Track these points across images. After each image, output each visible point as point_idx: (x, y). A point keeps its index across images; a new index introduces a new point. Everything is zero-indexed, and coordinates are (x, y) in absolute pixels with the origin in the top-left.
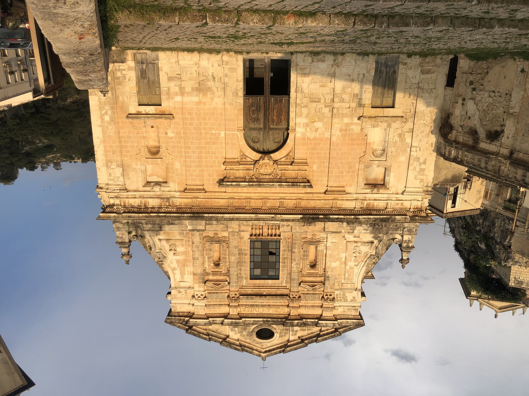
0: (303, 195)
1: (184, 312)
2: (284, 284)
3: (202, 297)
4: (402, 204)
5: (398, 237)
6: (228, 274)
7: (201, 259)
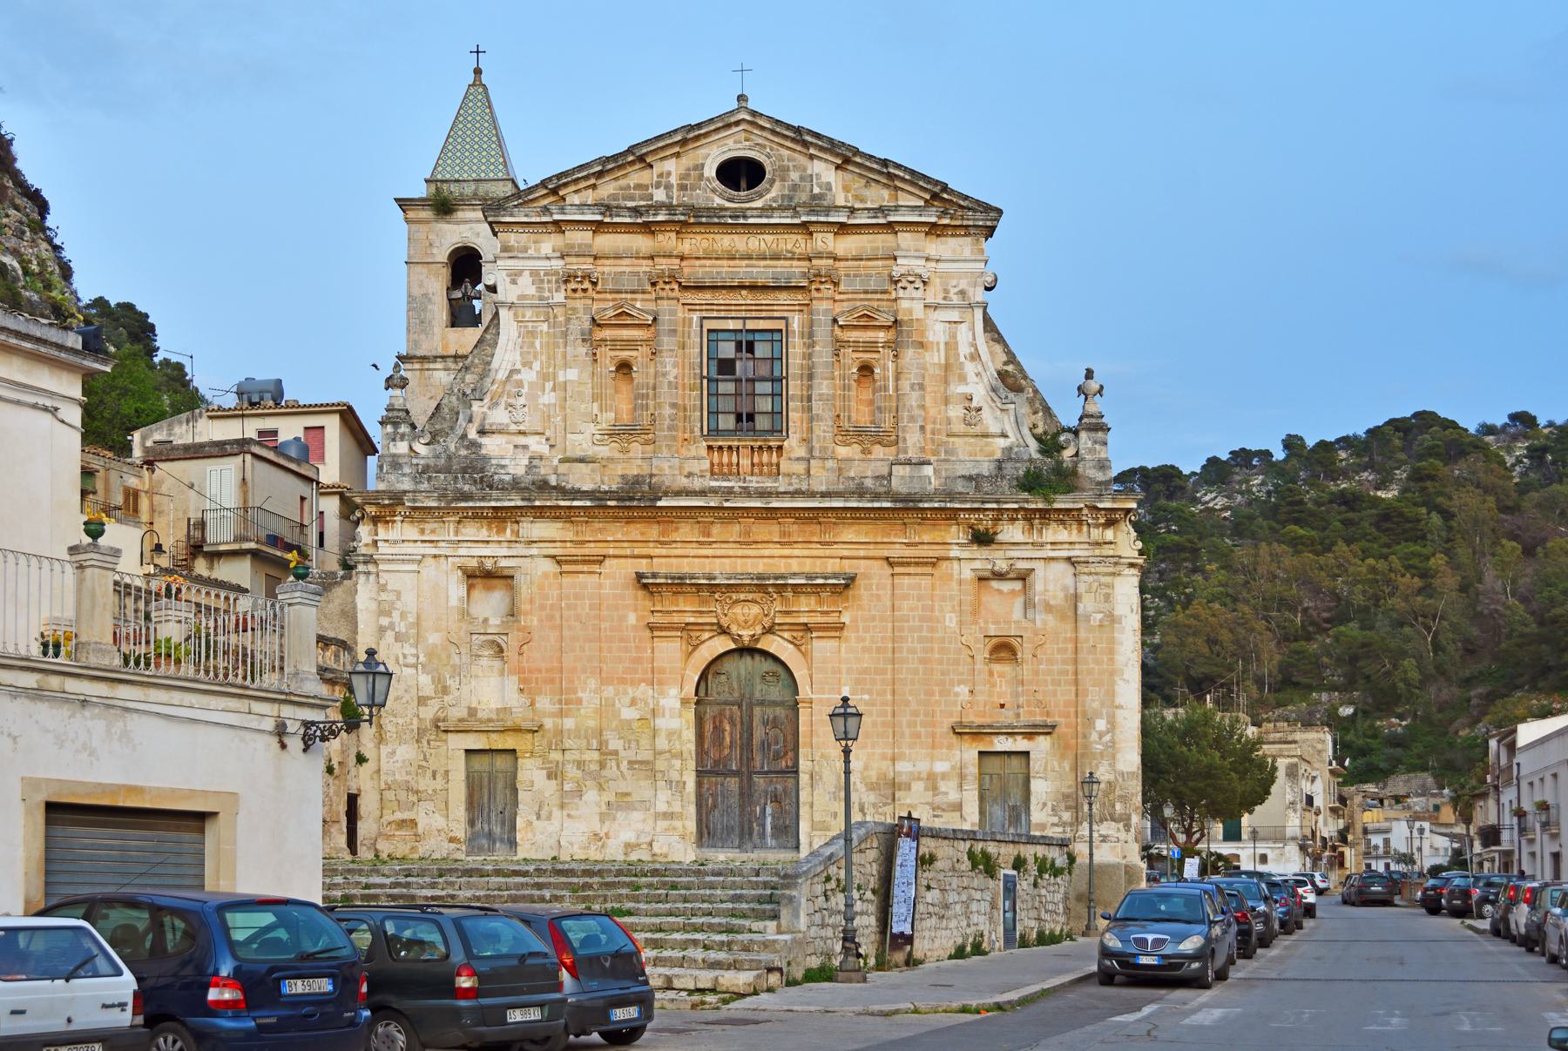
0: (657, 552)
1: (952, 235)
2: (695, 317)
3: (903, 283)
4: (422, 531)
5: (420, 448)
6: (839, 346)
7: (905, 385)
